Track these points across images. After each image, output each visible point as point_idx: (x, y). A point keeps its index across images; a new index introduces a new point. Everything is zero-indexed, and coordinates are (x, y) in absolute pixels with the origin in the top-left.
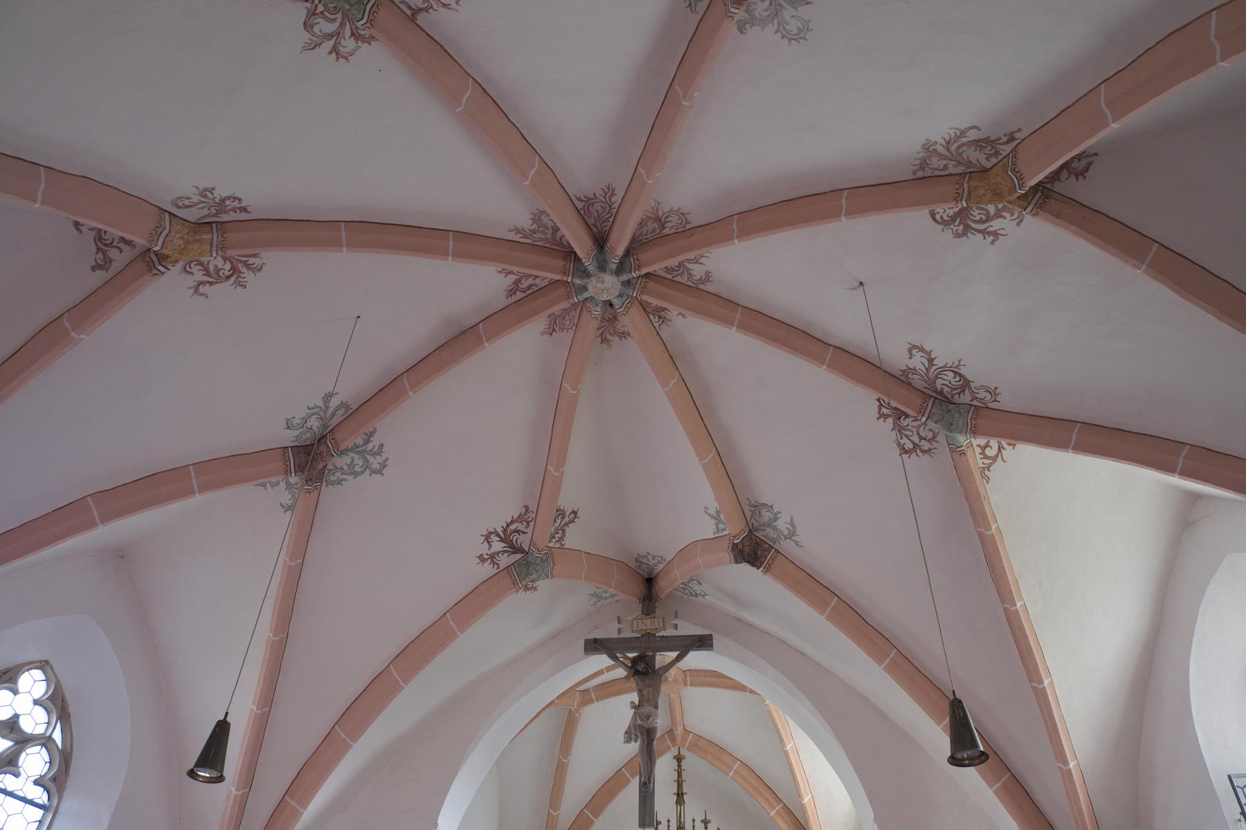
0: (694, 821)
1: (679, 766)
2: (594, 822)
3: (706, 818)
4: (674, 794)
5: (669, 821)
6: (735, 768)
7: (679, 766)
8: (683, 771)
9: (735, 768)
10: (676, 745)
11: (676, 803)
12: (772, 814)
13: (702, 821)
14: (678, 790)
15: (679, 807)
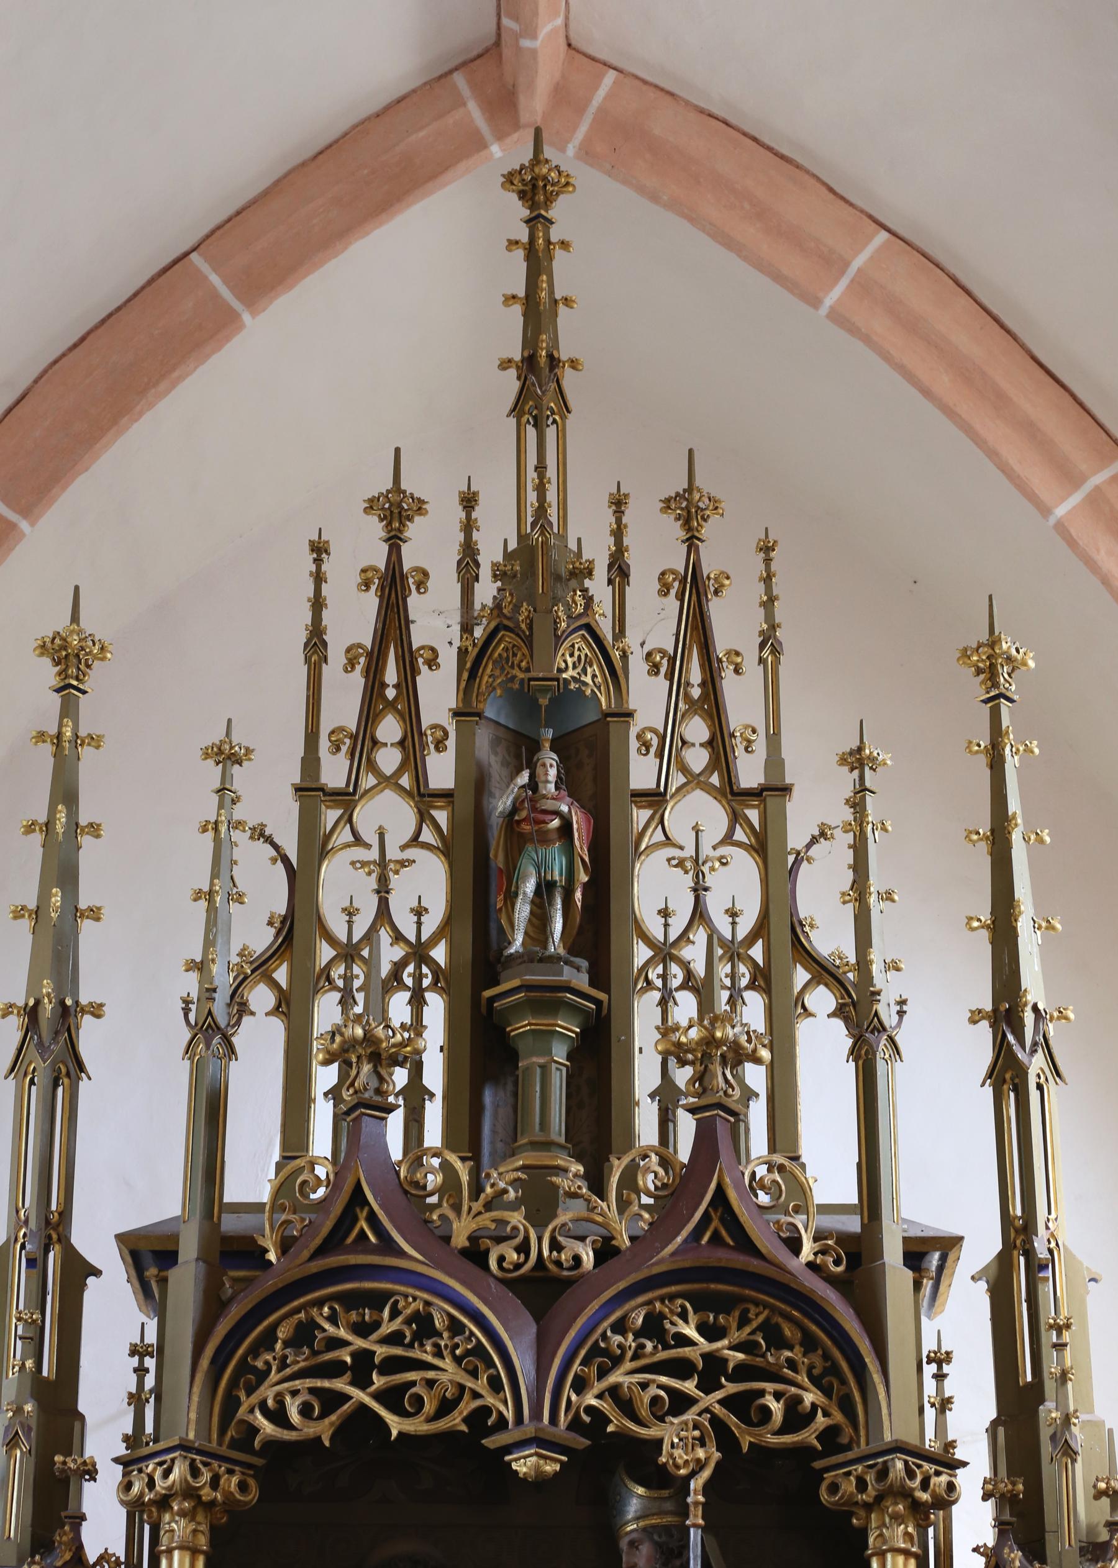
0: (619, 503)
1: (537, 221)
2: (23, 535)
3: (690, 489)
4: (505, 364)
5: (469, 501)
6: (858, 262)
7: (537, 221)
8: (559, 253)
9: (858, 262)
10: (517, 126)
11: (517, 409)
12: (1061, 511)
13: (667, 504)
14: (530, 341)
15: (531, 433)
